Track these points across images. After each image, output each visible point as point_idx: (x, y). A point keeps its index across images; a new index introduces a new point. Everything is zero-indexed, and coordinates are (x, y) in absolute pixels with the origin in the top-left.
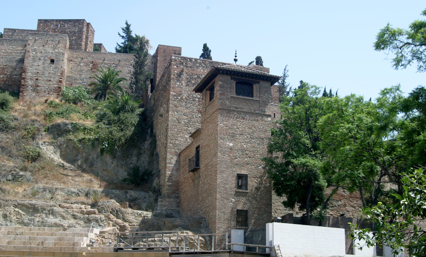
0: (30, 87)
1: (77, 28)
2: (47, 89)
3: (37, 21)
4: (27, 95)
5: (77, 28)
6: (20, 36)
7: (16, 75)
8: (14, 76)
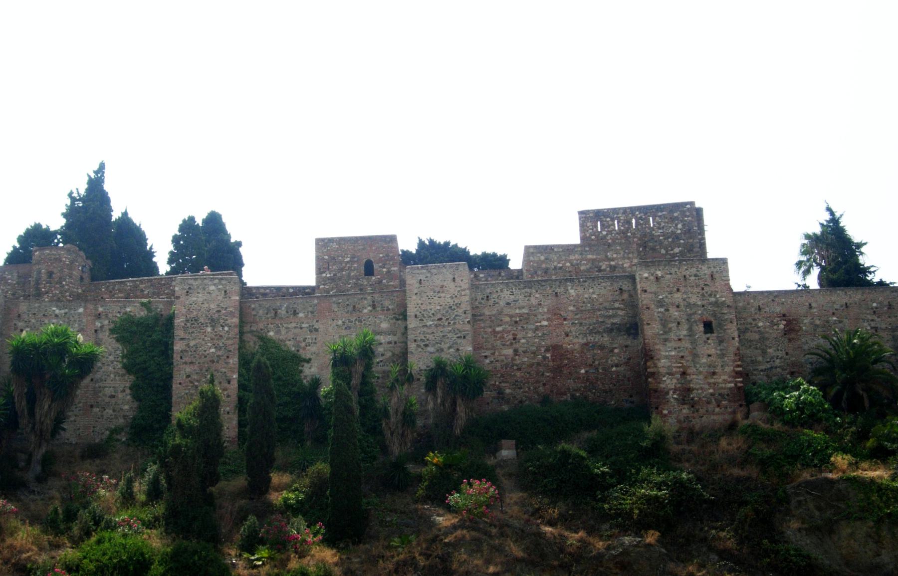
0: (671, 392)
1: (680, 226)
2: (712, 394)
3: (577, 216)
4: (670, 412)
5: (680, 226)
6: (566, 260)
7: (617, 366)
8: (614, 369)
